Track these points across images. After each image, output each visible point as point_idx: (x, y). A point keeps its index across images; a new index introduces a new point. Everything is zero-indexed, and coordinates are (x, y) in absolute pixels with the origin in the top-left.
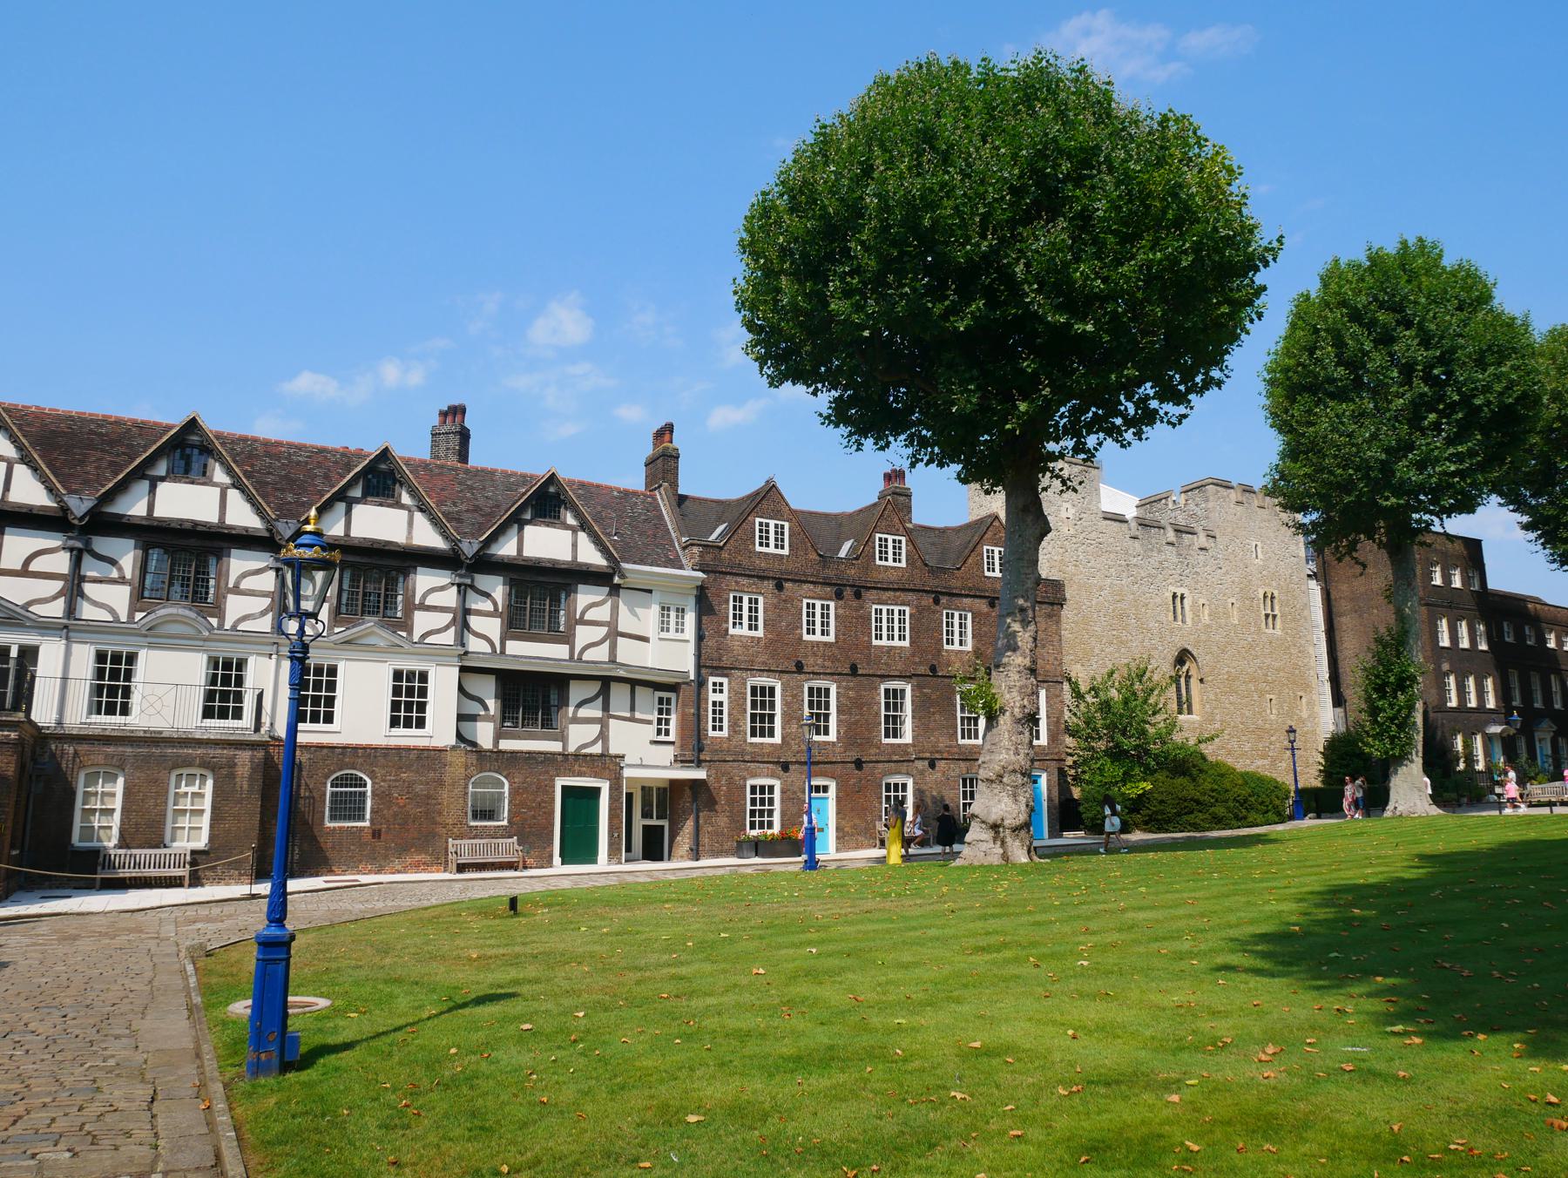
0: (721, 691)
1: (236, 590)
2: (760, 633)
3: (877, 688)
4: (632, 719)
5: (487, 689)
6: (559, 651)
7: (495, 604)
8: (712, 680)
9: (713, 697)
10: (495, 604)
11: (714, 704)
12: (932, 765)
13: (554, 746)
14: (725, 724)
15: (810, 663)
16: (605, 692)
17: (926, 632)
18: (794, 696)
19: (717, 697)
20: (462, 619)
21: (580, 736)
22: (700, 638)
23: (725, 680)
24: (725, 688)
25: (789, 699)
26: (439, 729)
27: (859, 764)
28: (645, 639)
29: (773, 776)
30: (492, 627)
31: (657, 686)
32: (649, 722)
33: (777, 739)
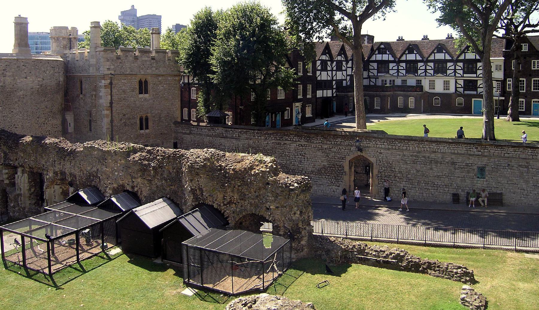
0: (510, 81)
1: (420, 69)
5: (461, 82)
6: (475, 75)
7: (461, 68)
8: (508, 79)
9: (508, 83)
10: (461, 68)
11: (508, 84)
13: (475, 93)
14: (511, 88)
19: (509, 83)
20: (455, 71)
22: (505, 70)
23: (511, 79)
24: (511, 81)
25: (528, 83)
26: (452, 90)
29: (523, 98)
31: (497, 81)
33: (525, 91)
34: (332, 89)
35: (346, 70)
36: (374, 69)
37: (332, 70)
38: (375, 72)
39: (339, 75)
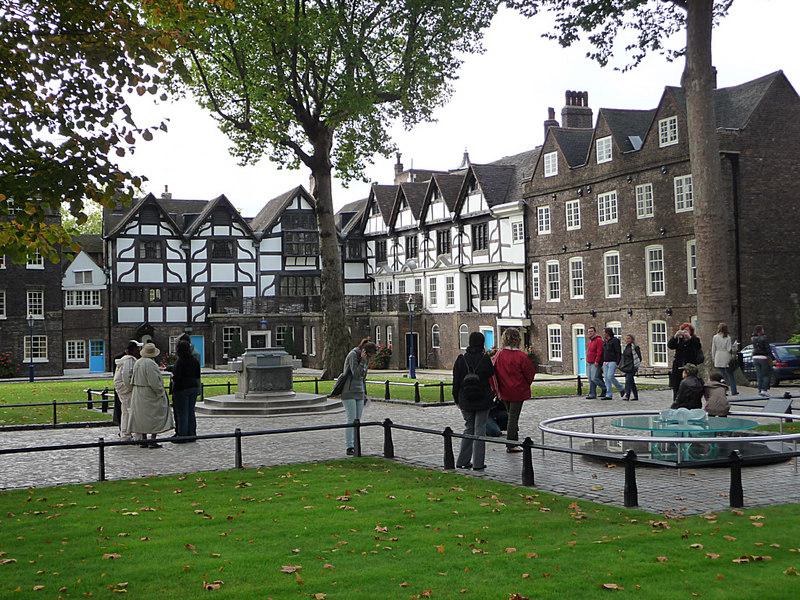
2: (549, 232)
3: (600, 258)
4: (518, 292)
5: (476, 280)
8: (534, 264)
12: (631, 313)
15: (571, 245)
16: (509, 278)
17: (627, 207)
18: (564, 270)
21: (503, 300)
23: (537, 264)
27: (594, 314)
28: (509, 246)
30: (468, 250)
32: (521, 292)
34: (190, 304)
35: (256, 261)
36: (372, 257)
37: (189, 261)
38: (372, 262)
39: (223, 273)
